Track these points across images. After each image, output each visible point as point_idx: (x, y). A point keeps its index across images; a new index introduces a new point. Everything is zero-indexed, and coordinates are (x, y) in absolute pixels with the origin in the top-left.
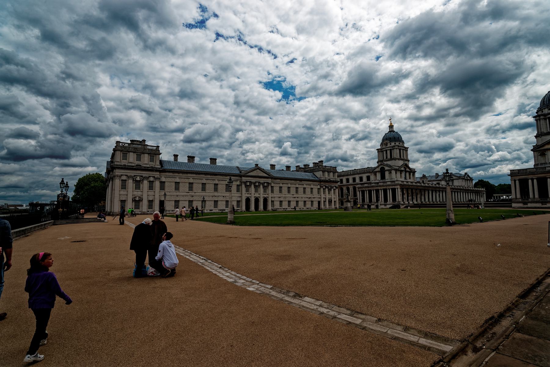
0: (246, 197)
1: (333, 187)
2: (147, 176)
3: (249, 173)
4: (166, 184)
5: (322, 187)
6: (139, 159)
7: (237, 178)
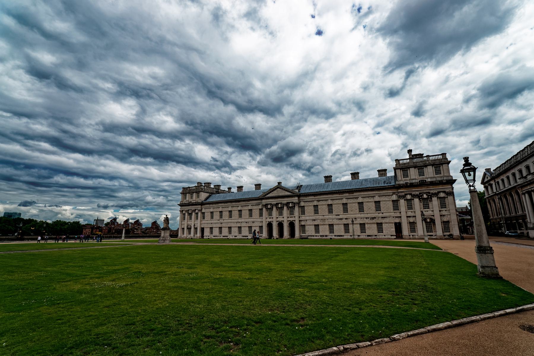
0: (268, 222)
1: (436, 194)
2: (194, 209)
3: (267, 194)
4: (206, 214)
5: (404, 197)
6: (192, 198)
7: (259, 201)
